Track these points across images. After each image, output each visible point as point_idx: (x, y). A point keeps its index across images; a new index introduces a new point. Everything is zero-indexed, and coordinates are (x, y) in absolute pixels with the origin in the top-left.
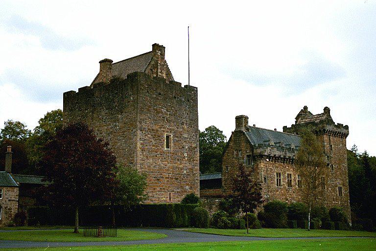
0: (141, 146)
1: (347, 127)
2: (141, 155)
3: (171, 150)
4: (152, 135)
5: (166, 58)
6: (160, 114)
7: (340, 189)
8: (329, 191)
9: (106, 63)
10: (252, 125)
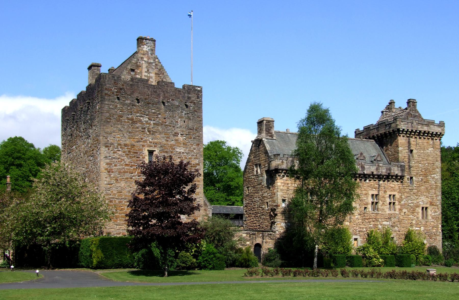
0: (106, 167)
1: (442, 125)
2: (106, 178)
4: (124, 152)
5: (157, 53)
6: (138, 125)
7: (425, 209)
8: (403, 214)
10: (283, 130)
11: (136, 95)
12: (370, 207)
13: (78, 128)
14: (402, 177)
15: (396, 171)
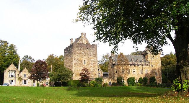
3: (86, 64)
5: (86, 36)
9: (72, 39)
11: (81, 47)
12: (140, 73)
13: (68, 54)
14: (149, 65)
15: (147, 63)
